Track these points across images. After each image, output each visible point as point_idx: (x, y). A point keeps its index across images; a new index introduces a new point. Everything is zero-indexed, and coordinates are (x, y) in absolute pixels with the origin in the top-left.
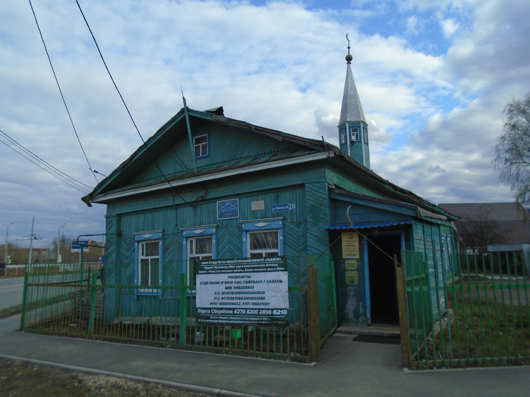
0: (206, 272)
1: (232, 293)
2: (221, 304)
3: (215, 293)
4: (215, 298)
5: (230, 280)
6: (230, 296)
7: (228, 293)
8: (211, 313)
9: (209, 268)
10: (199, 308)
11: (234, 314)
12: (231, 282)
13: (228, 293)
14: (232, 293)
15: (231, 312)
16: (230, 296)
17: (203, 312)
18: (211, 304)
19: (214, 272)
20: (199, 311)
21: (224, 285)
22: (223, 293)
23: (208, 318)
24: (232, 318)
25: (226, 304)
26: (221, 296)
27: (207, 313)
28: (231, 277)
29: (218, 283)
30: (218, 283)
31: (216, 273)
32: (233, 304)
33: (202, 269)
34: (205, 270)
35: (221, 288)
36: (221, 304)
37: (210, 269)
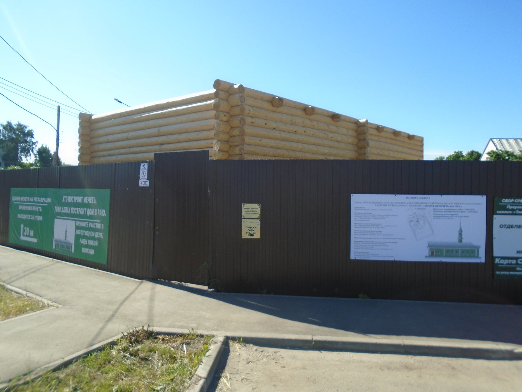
0: (510, 212)
8: (517, 264)
9: (515, 208)
10: (498, 257)
17: (506, 262)
20: (497, 261)
23: (514, 270)
27: (511, 264)
33: (504, 208)
34: (509, 210)
37: (517, 209)
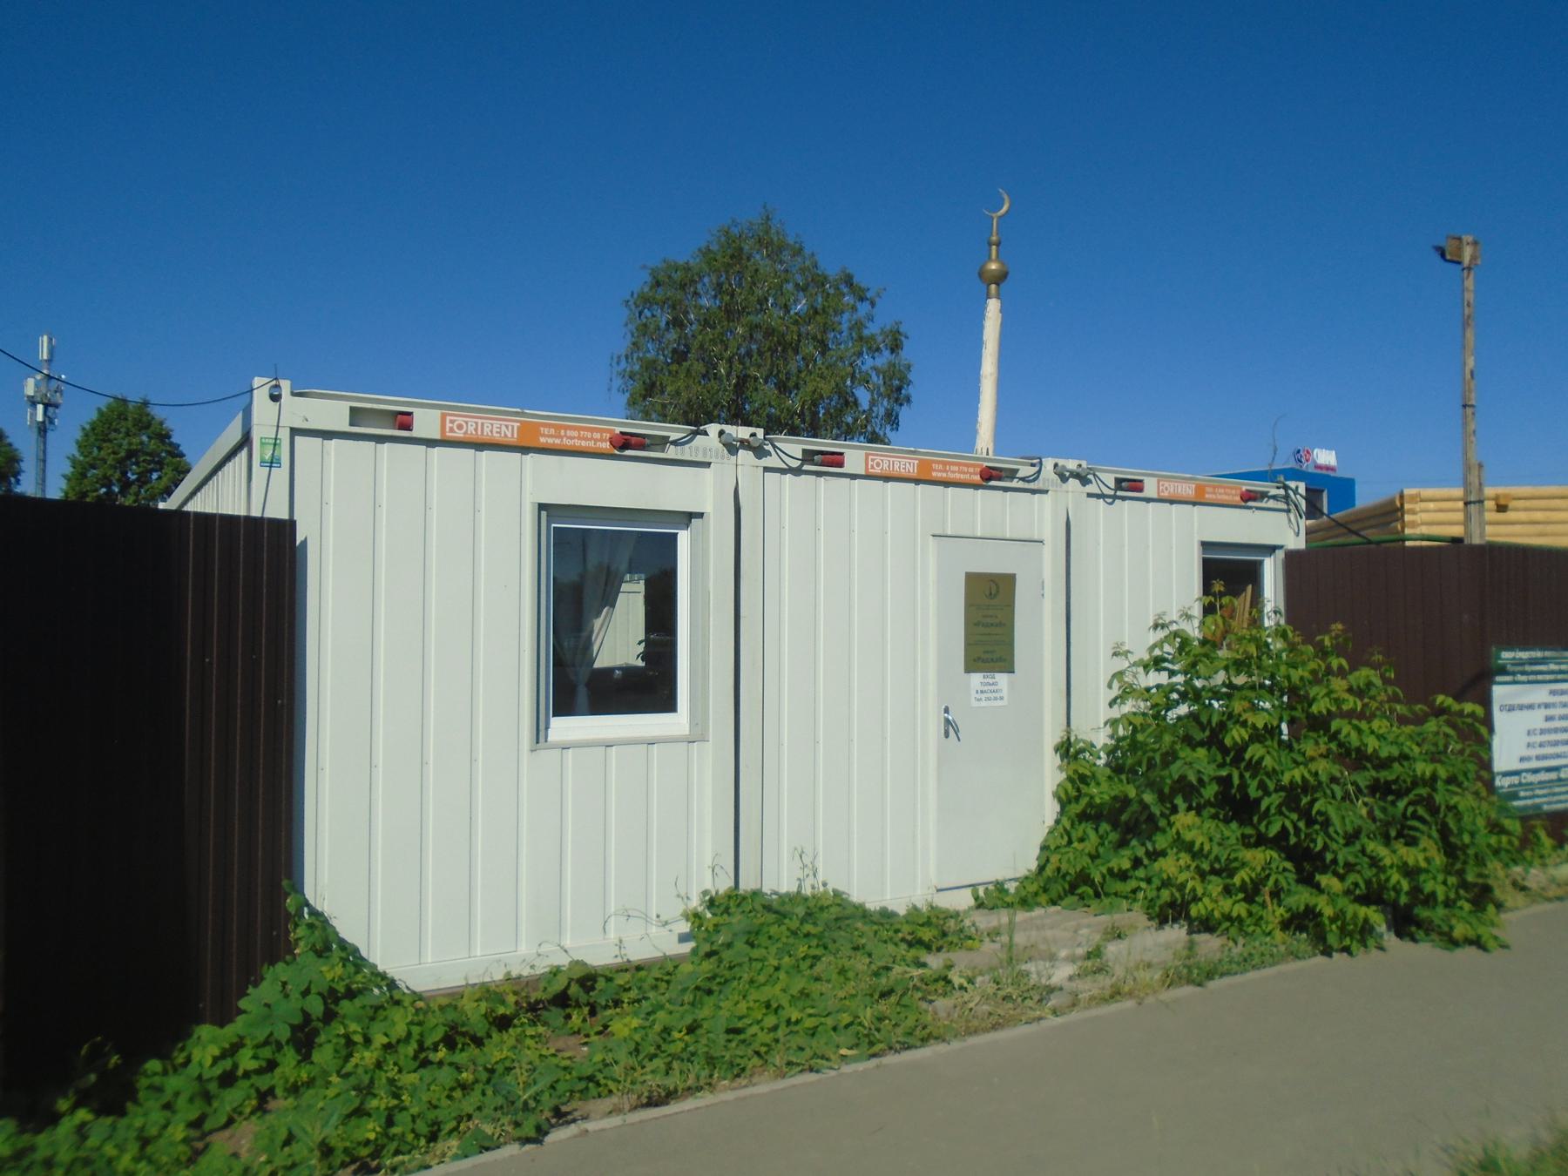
1: (1556, 730)
2: (1538, 758)
3: (1529, 733)
4: (1529, 745)
5: (1552, 699)
6: (1553, 737)
7: (1549, 731)
11: (1560, 780)
12: (1553, 705)
13: (1549, 731)
14: (1556, 730)
15: (1553, 775)
16: (1553, 737)
18: (1522, 759)
19: (1524, 678)
21: (1544, 712)
22: (1543, 732)
24: (1557, 790)
25: (1545, 757)
26: (1539, 739)
28: (1553, 693)
29: (1530, 707)
30: (1530, 707)
31: (1529, 682)
32: (1558, 756)
35: (1536, 719)
36: (1538, 758)
